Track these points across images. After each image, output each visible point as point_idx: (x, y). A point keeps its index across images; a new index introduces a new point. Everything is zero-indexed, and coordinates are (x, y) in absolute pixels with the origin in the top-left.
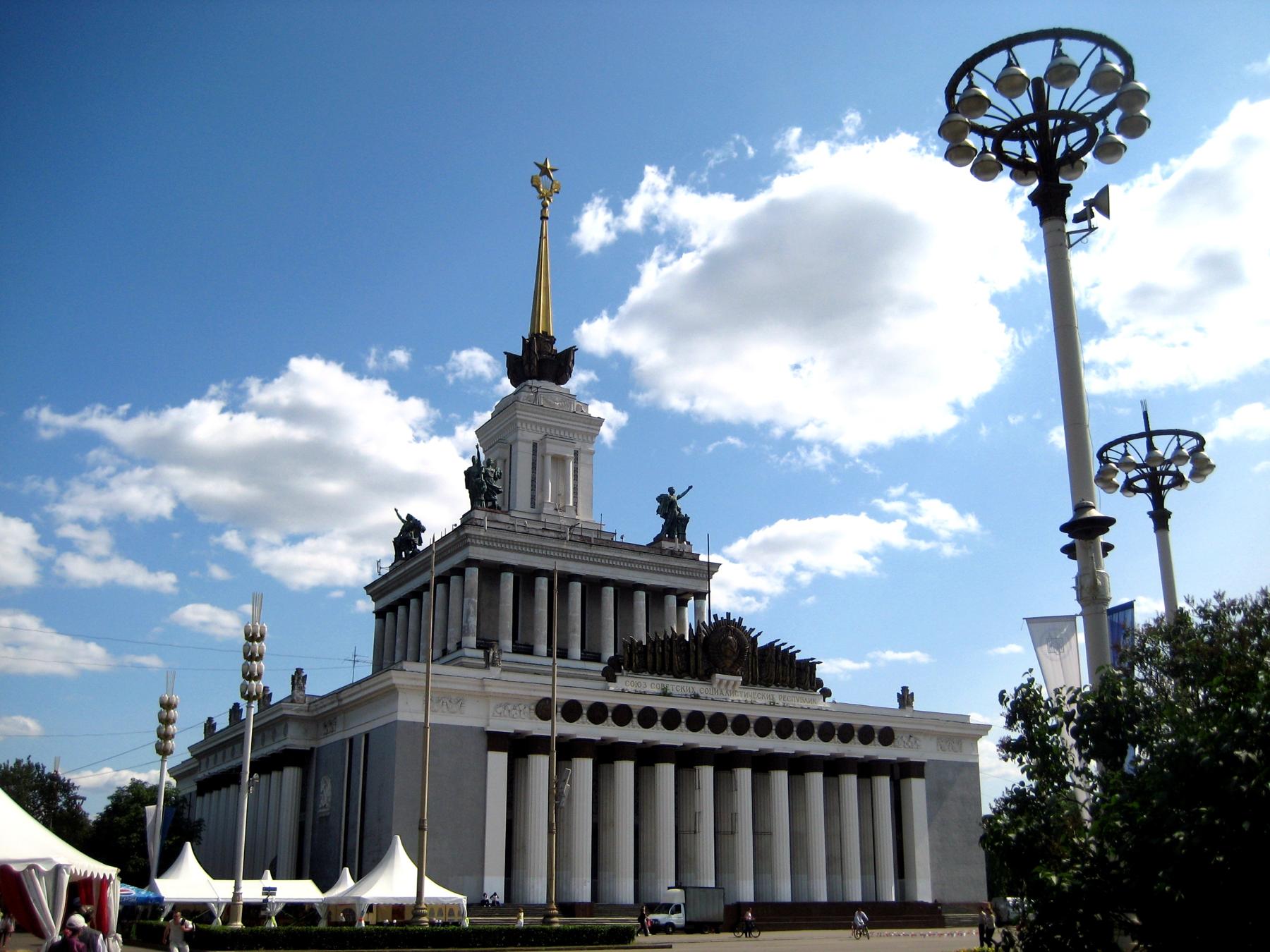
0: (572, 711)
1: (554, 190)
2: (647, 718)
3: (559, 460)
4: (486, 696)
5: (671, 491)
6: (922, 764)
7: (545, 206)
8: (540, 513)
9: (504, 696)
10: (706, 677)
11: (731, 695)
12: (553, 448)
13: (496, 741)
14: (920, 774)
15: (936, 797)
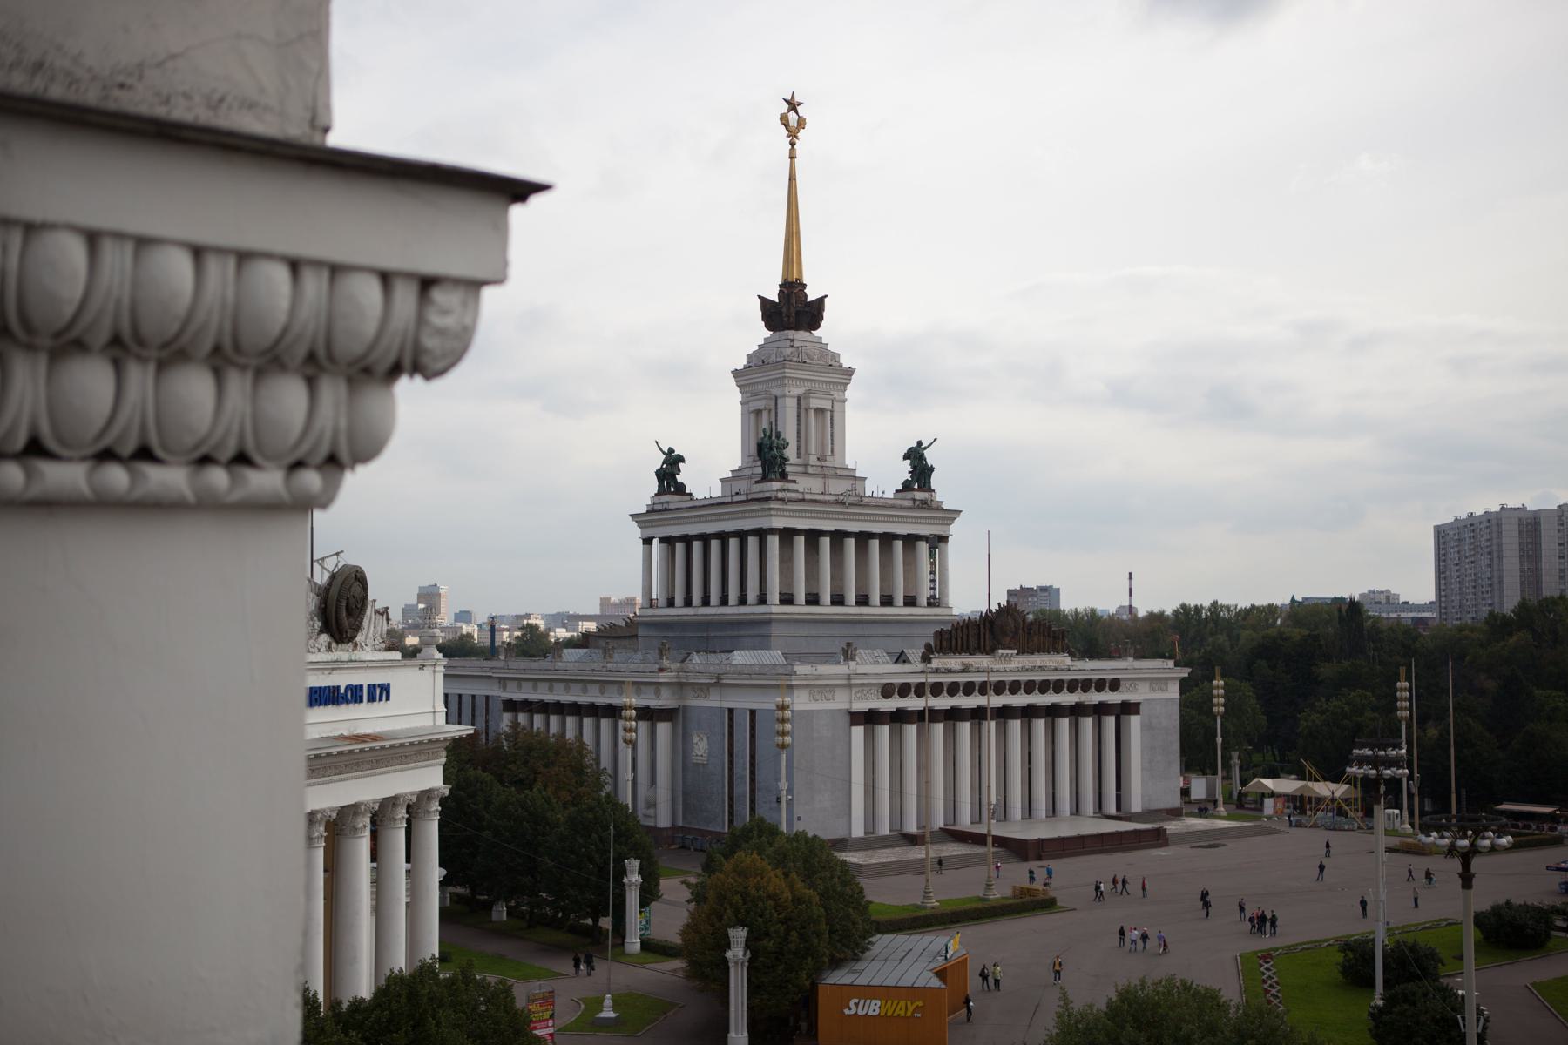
0: (904, 690)
1: (801, 123)
2: (953, 689)
3: (820, 411)
4: (850, 686)
5: (920, 443)
6: (1138, 704)
7: (793, 144)
8: (806, 465)
9: (863, 685)
10: (990, 651)
11: (1009, 664)
12: (815, 403)
13: (856, 718)
14: (1138, 713)
15: (1146, 727)
